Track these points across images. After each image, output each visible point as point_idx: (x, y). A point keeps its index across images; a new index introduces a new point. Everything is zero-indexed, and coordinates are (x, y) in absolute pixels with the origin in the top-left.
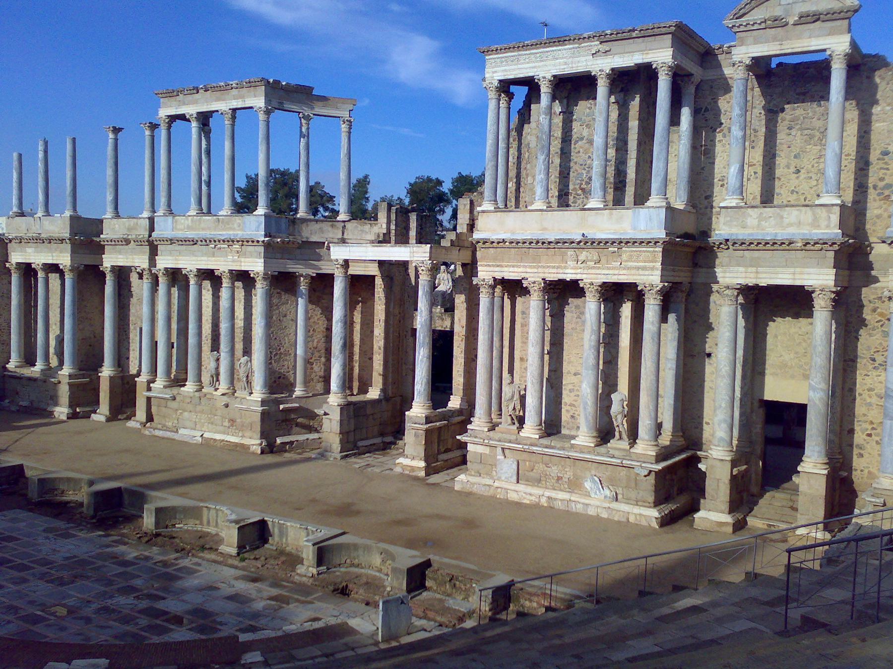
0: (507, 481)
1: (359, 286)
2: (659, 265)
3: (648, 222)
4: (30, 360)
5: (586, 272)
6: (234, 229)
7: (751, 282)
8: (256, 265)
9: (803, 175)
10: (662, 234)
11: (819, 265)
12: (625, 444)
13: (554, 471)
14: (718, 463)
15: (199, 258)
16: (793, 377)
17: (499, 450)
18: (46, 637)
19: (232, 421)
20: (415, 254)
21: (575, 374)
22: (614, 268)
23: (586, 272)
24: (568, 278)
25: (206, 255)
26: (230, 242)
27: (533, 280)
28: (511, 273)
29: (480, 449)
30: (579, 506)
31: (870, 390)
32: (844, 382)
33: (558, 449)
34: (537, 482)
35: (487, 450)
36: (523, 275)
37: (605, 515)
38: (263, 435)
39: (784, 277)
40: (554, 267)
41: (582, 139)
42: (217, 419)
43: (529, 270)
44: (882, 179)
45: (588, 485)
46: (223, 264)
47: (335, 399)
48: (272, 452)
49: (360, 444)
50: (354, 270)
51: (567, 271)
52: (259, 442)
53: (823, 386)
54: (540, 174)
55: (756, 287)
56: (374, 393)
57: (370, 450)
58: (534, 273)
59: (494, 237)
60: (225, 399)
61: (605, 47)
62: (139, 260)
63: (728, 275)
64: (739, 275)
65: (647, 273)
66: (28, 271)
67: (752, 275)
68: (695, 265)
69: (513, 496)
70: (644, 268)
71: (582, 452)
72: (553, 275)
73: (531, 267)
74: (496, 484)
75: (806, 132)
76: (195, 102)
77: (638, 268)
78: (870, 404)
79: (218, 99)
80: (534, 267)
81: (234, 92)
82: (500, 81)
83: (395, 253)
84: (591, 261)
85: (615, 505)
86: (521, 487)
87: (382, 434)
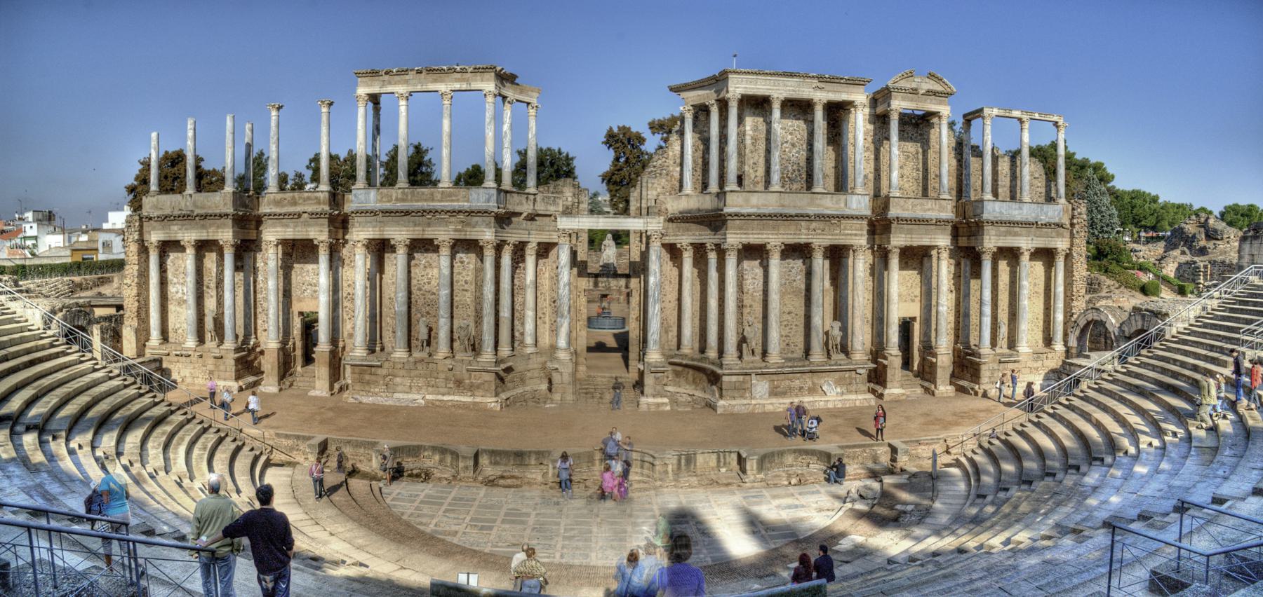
0: (761, 398)
2: (865, 232)
3: (859, 203)
6: (458, 200)
7: (908, 244)
10: (868, 213)
12: (842, 356)
13: (797, 383)
28: (754, 238)
29: (734, 378)
34: (783, 394)
35: (741, 378)
39: (925, 241)
42: (441, 382)
52: (494, 399)
61: (821, 85)
69: (770, 408)
76: (406, 82)
79: (435, 81)
81: (458, 76)
82: (743, 96)
86: (774, 400)
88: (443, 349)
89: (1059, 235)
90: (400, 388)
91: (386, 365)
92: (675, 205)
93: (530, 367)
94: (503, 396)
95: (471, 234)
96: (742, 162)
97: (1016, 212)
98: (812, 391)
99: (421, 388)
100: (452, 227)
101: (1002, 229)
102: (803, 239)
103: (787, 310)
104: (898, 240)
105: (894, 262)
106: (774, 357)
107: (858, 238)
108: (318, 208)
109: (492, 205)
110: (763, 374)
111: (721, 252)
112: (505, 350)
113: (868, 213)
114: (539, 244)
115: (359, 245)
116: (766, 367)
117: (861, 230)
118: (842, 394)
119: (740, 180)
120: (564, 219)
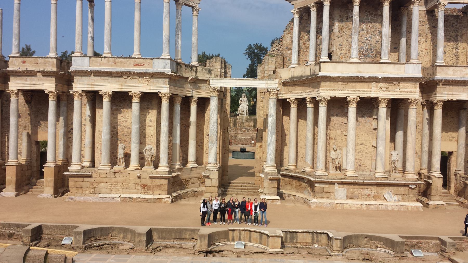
5: (381, 93)
7: (450, 99)
8: (163, 88)
13: (367, 190)
15: (113, 84)
17: (336, 184)
19: (144, 186)
21: (361, 144)
22: (397, 91)
23: (381, 93)
25: (119, 81)
26: (141, 75)
27: (354, 97)
28: (340, 93)
30: (383, 207)
33: (368, 180)
34: (357, 198)
36: (347, 95)
37: (396, 209)
40: (364, 91)
41: (363, 30)
42: (132, 185)
43: (350, 92)
46: (135, 87)
51: (371, 93)
54: (356, 44)
58: (354, 93)
59: (333, 74)
60: (138, 173)
63: (440, 95)
64: (445, 95)
65: (412, 94)
67: (450, 96)
70: (411, 92)
71: (381, 180)
72: (364, 95)
73: (352, 91)
74: (336, 202)
75: (448, 37)
77: (408, 92)
80: (354, 91)
84: (385, 87)
86: (350, 201)
90: (104, 190)
91: (94, 175)
92: (285, 74)
93: (192, 176)
94: (174, 194)
95: (153, 89)
96: (330, 44)
98: (376, 198)
99: (118, 190)
100: (141, 84)
102: (373, 95)
103: (360, 142)
104: (443, 95)
105: (438, 112)
107: (412, 93)
108: (49, 69)
109: (168, 71)
110: (343, 183)
111: (316, 103)
113: (421, 76)
114: (199, 98)
115: (77, 94)
116: (345, 179)
117: (415, 88)
119: (330, 56)
120: (215, 80)
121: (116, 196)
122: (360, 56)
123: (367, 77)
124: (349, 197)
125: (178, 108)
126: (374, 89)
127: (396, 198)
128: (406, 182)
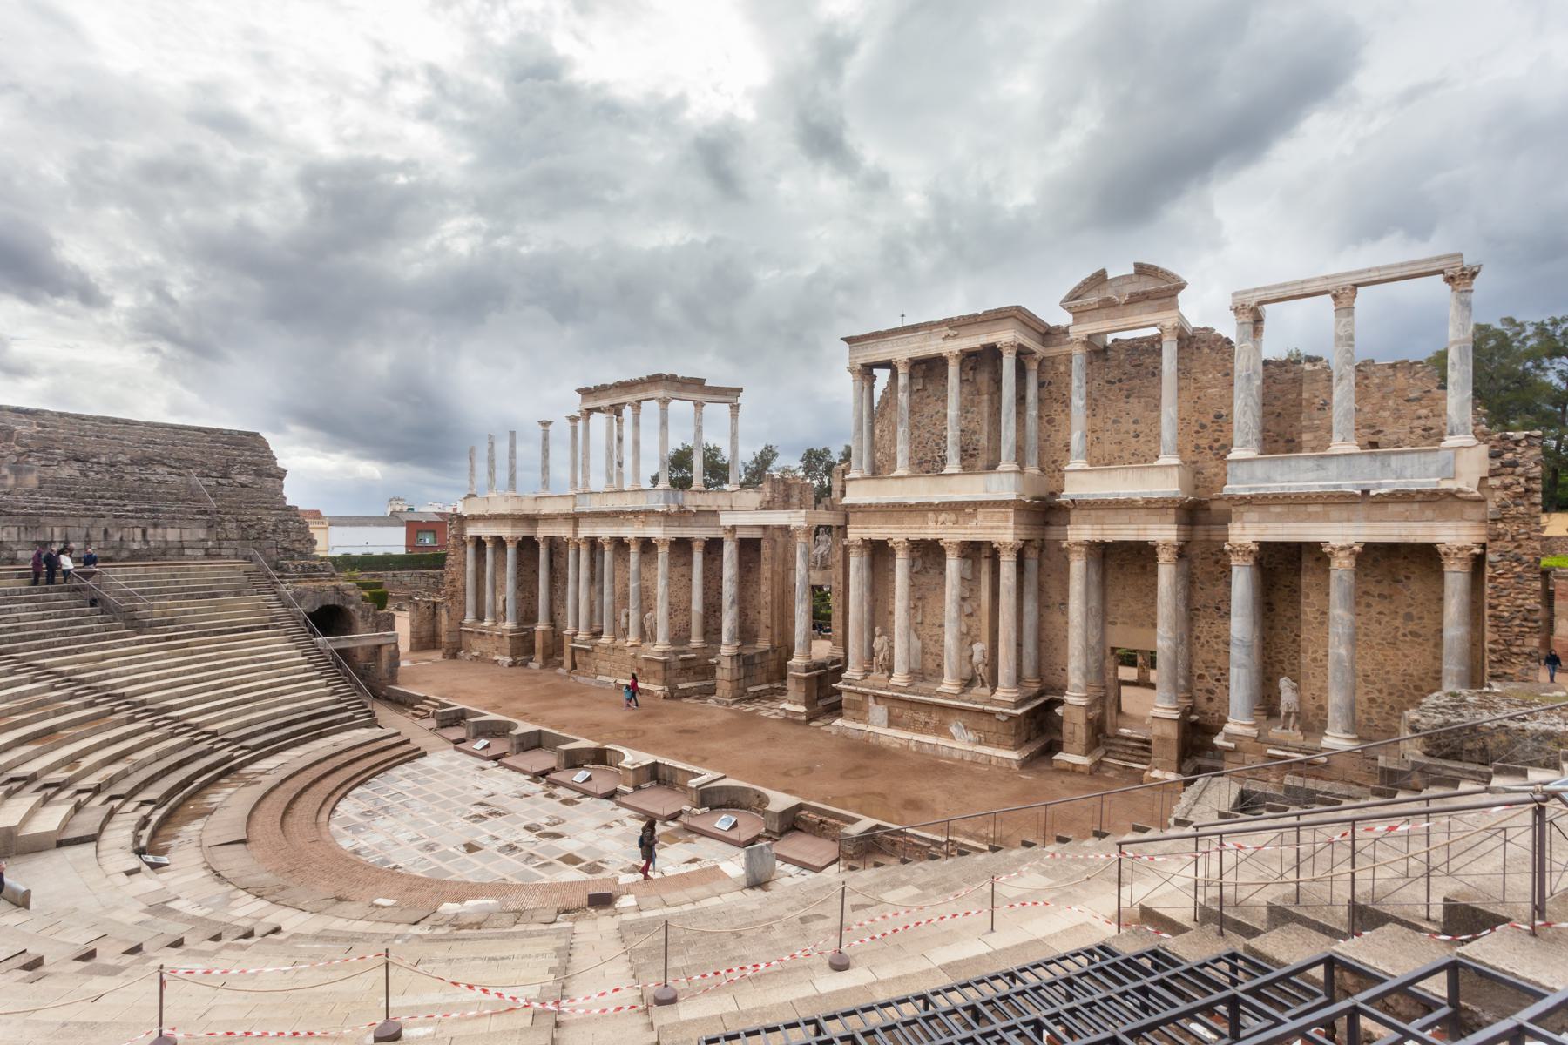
1: (749, 548)
2: (1011, 524)
4: (480, 617)
7: (1097, 538)
8: (656, 532)
9: (1142, 439)
11: (1161, 522)
13: (922, 717)
14: (1074, 709)
16: (1142, 626)
17: (871, 699)
18: (450, 874)
20: (795, 519)
24: (929, 537)
26: (635, 513)
28: (877, 532)
29: (854, 697)
31: (1217, 637)
32: (1191, 630)
34: (906, 727)
35: (860, 698)
38: (665, 682)
44: (1217, 441)
45: (953, 730)
46: (630, 532)
47: (727, 649)
48: (672, 697)
49: (751, 689)
50: (741, 534)
53: (1170, 634)
55: (1103, 543)
56: (763, 644)
57: (758, 696)
62: (563, 531)
66: (479, 543)
68: (1047, 523)
72: (916, 535)
74: (870, 729)
78: (1218, 651)
79: (627, 393)
83: (778, 518)
85: (979, 749)
86: (893, 732)
87: (769, 681)
88: (633, 638)
89: (1446, 518)
97: (1311, 475)
101: (1278, 509)
102: (930, 534)
105: (1077, 566)
106: (899, 678)
112: (696, 642)
113: (1010, 495)
116: (887, 688)
118: (979, 743)
121: (611, 680)
122: (911, 464)
123: (912, 501)
124: (891, 723)
125: (698, 557)
126: (931, 524)
127: (971, 736)
128: (987, 708)
